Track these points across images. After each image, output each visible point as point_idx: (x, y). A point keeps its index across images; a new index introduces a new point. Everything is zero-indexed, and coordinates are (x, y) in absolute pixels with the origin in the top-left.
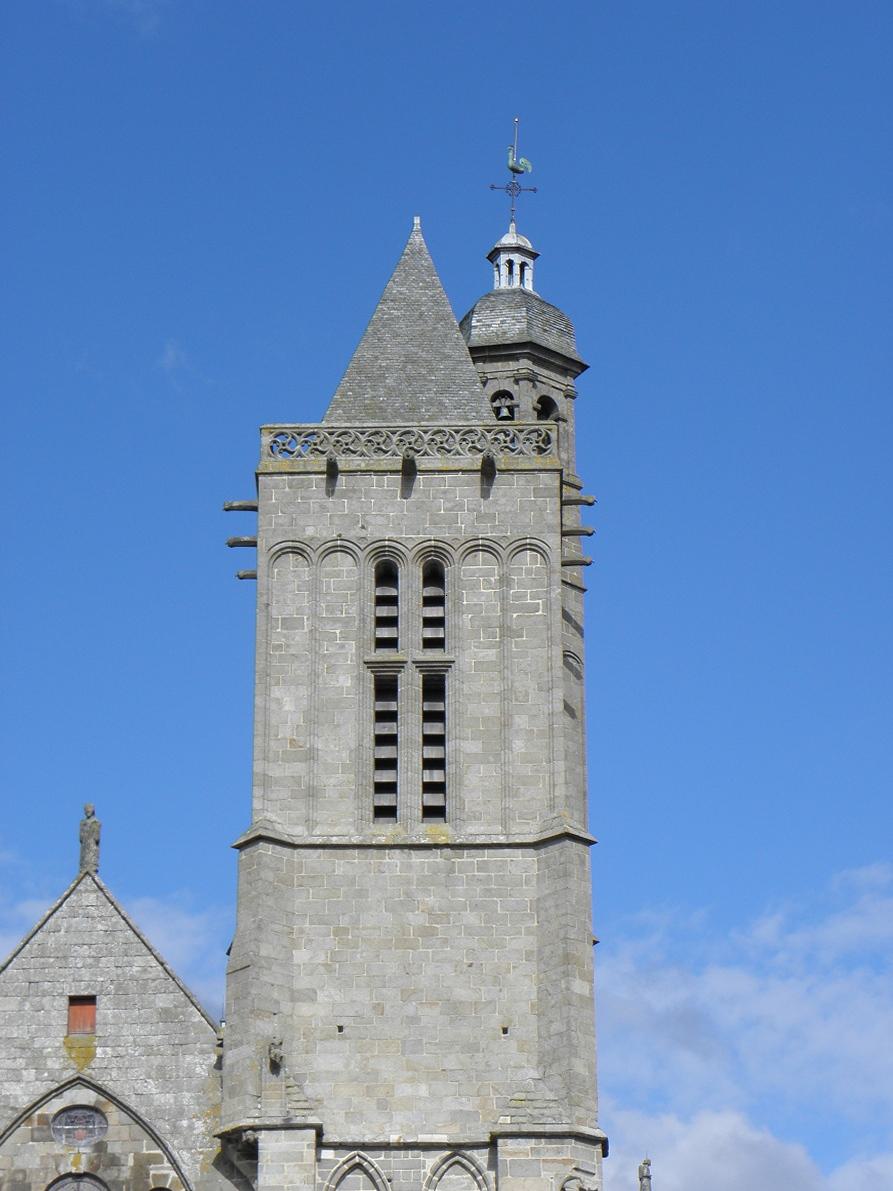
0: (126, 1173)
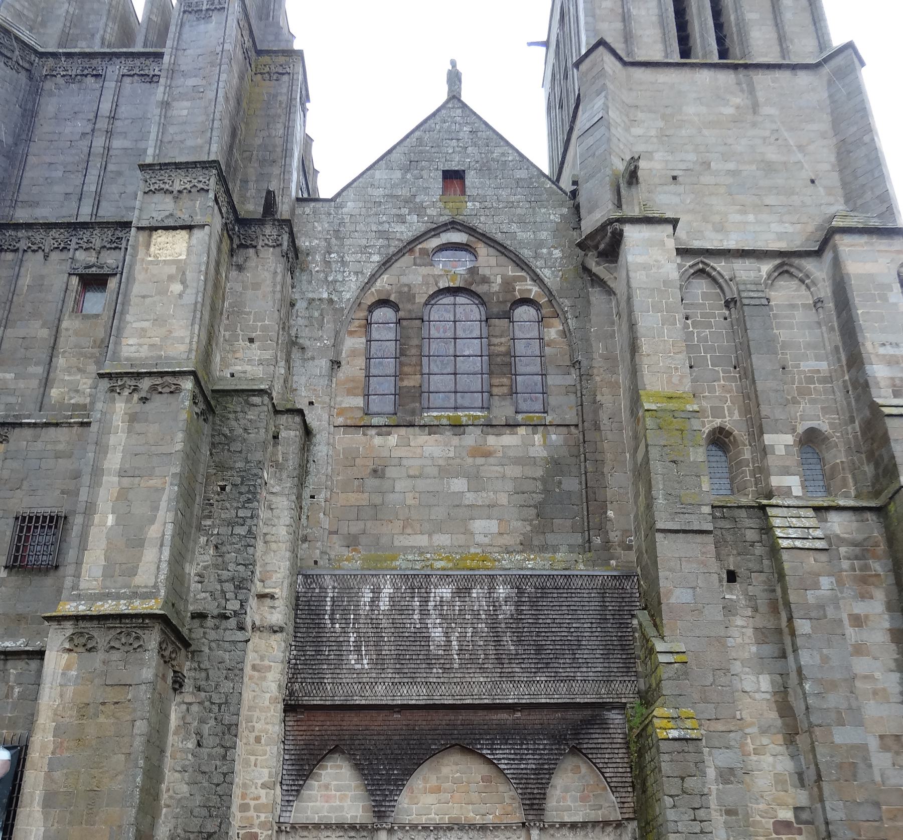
0: (495, 288)
